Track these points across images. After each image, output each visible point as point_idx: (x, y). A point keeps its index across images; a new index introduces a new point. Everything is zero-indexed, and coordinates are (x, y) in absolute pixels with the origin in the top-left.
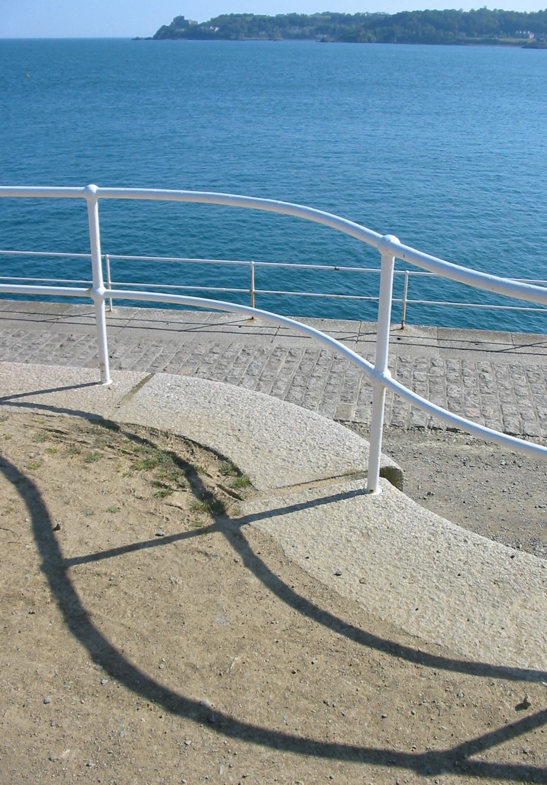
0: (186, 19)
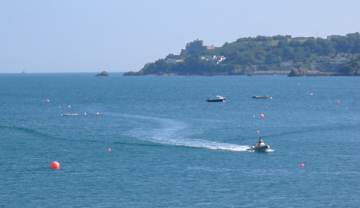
0: (204, 44)
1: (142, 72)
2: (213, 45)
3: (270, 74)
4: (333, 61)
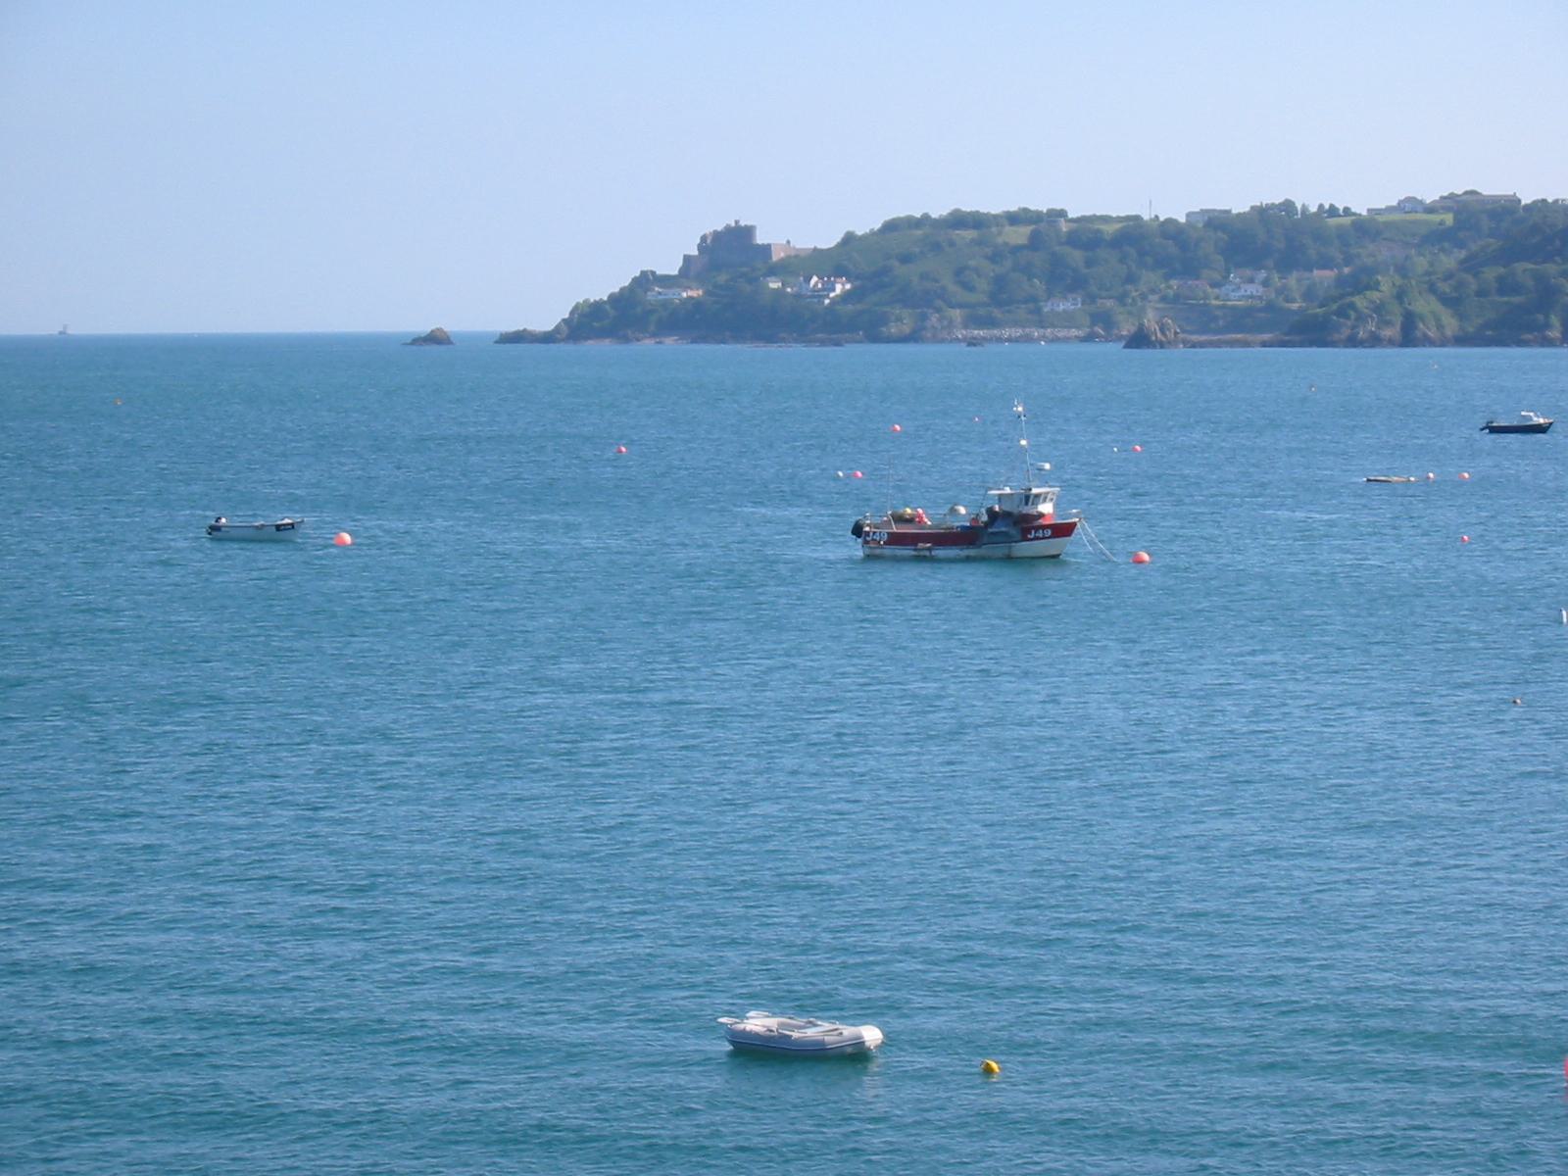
0: (760, 239)
1: (565, 330)
2: (788, 242)
3: (1009, 340)
4: (1217, 298)
